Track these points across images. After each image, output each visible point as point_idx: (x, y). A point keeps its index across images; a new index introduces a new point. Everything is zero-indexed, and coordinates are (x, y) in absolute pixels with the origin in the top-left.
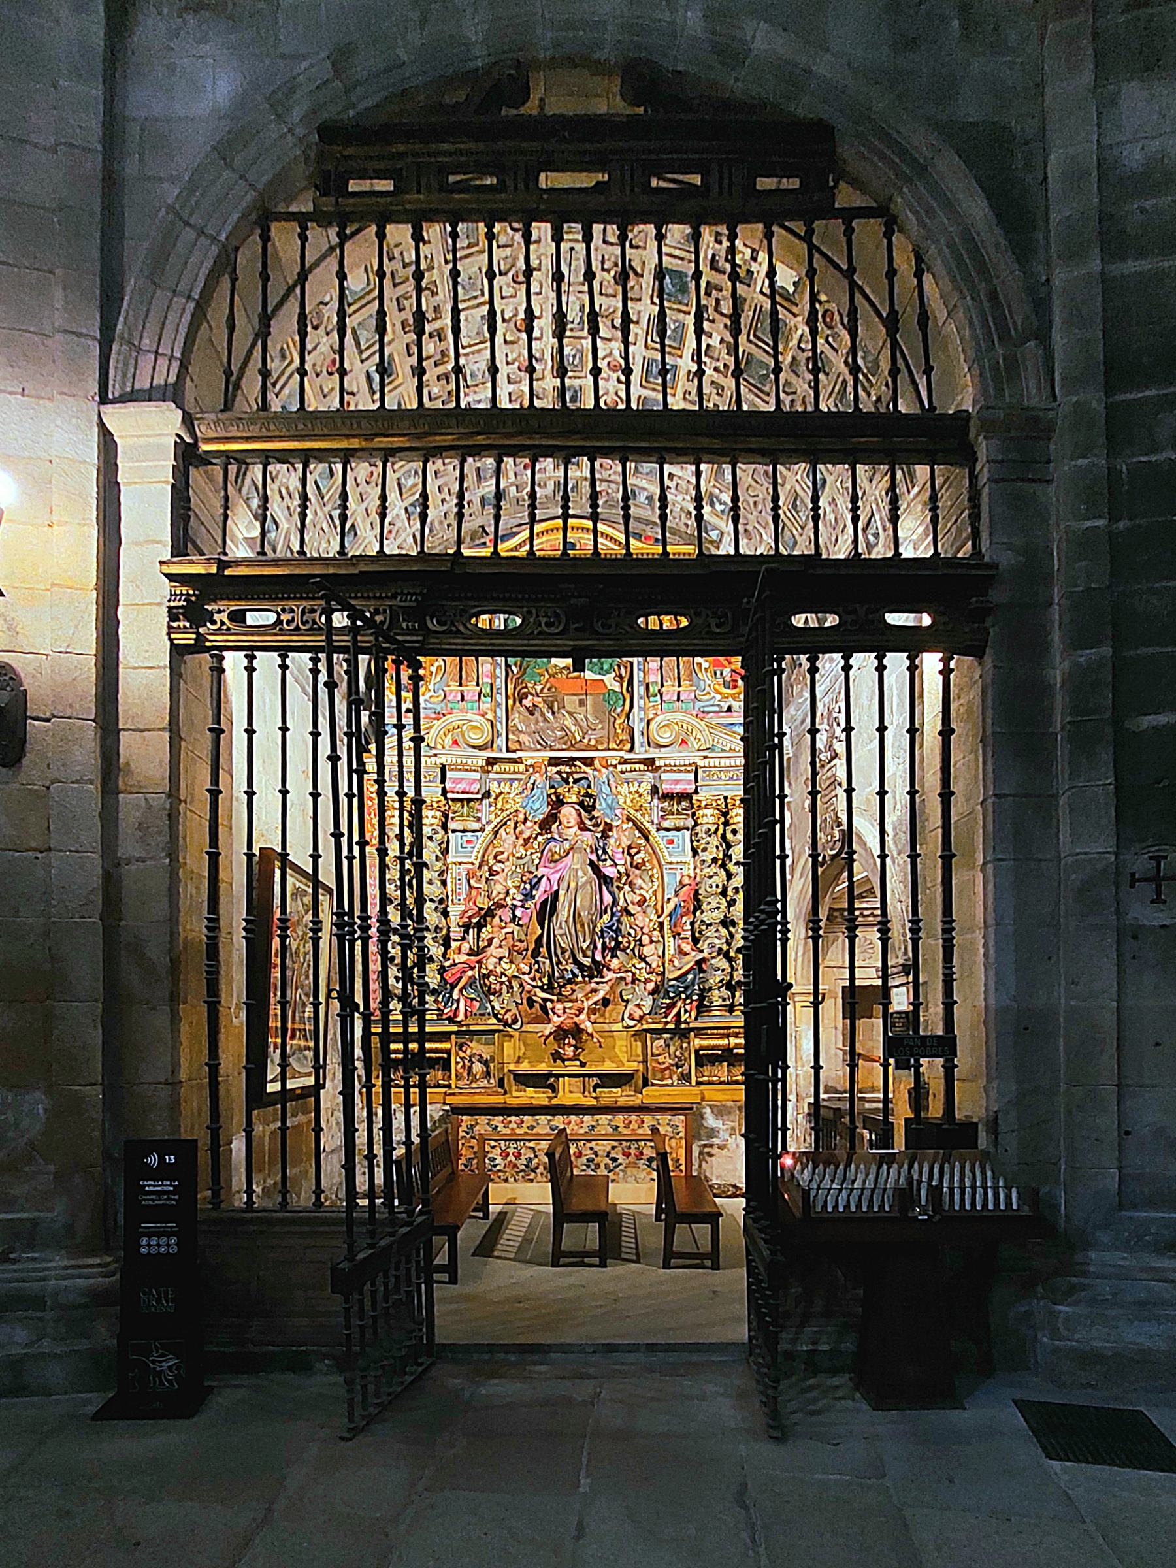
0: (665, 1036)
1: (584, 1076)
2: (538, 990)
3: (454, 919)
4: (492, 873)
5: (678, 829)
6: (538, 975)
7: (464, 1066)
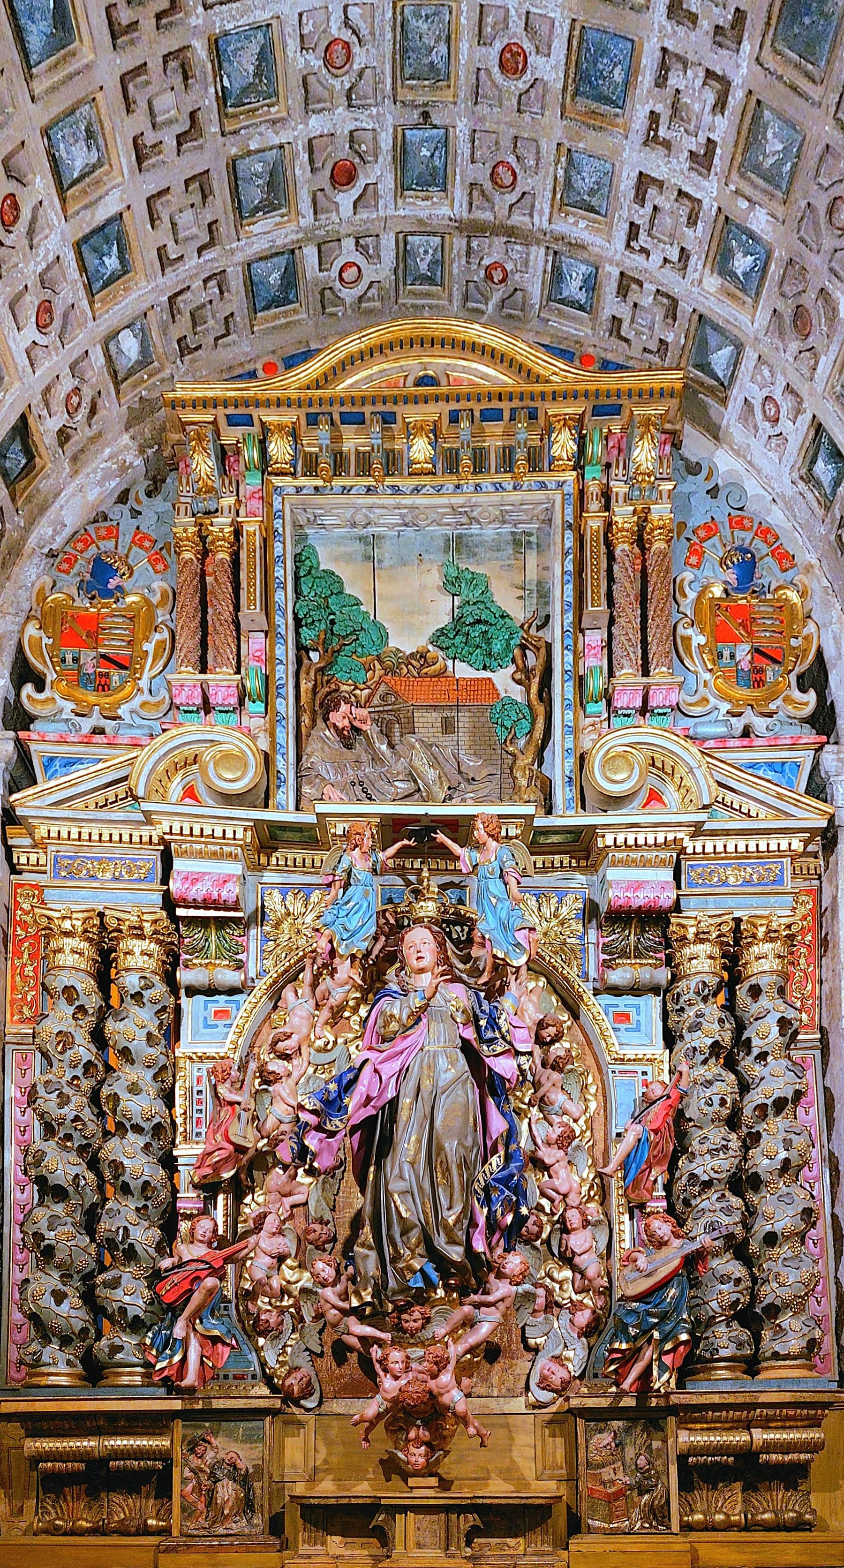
0: (617, 1424)
1: (447, 1509)
2: (352, 1321)
3: (184, 1175)
4: (268, 1079)
5: (636, 990)
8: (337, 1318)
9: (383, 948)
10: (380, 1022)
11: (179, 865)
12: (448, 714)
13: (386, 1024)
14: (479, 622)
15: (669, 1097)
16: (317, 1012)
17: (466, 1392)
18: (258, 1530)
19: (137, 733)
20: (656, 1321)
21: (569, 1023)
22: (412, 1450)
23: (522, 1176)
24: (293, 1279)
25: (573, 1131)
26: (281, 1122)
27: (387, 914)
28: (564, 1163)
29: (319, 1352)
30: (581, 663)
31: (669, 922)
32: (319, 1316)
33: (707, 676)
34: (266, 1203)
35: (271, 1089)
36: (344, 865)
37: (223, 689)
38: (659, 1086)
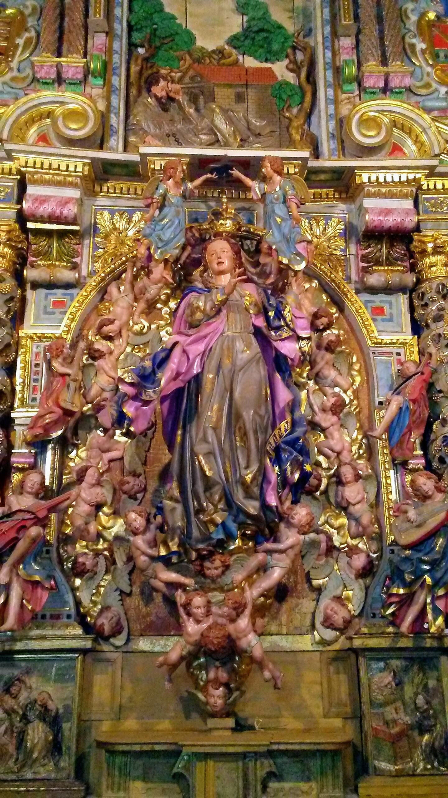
0: (396, 663)
2: (159, 566)
6: (160, 536)
7: (10, 730)
9: (189, 255)
11: (31, 190)
12: (240, 90)
13: (193, 314)
14: (262, 30)
15: (422, 373)
16: (135, 304)
17: (259, 631)
18: (64, 774)
19: (6, 97)
20: (427, 568)
21: (337, 315)
22: (212, 691)
23: (306, 439)
25: (344, 400)
26: (103, 390)
27: (194, 230)
28: (337, 427)
30: (337, 59)
31: (411, 240)
32: (130, 558)
33: (429, 69)
34: (89, 458)
36: (161, 191)
37: (73, 69)
38: (412, 364)
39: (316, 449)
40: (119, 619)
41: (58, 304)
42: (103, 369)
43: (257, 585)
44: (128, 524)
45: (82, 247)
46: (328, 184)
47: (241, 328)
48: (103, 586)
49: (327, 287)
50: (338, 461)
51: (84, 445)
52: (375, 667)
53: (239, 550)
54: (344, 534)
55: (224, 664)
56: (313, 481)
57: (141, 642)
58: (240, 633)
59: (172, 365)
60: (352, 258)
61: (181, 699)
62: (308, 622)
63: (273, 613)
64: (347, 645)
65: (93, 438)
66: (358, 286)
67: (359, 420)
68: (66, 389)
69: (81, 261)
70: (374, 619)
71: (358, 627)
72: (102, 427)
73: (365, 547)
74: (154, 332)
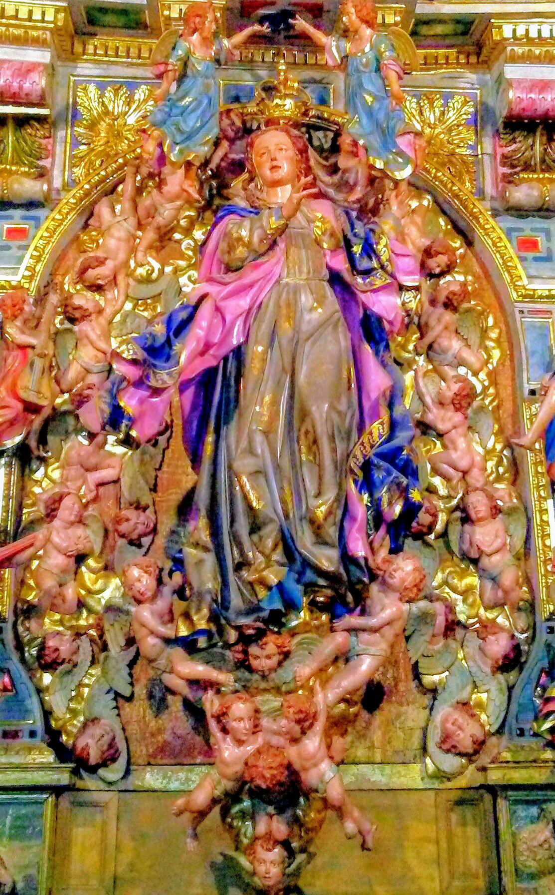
2: (178, 652)
6: (180, 606)
8: (158, 649)
9: (226, 155)
10: (223, 246)
13: (231, 249)
16: (140, 233)
17: (338, 758)
21: (462, 251)
23: (412, 450)
24: (97, 586)
25: (473, 388)
26: (88, 371)
29: (127, 693)
32: (131, 641)
34: (64, 480)
35: (76, 328)
39: (429, 466)
40: (114, 739)
41: (13, 233)
42: (87, 337)
43: (334, 683)
44: (127, 586)
45: (54, 142)
46: (448, 41)
47: (309, 273)
48: (87, 686)
49: (446, 207)
50: (464, 485)
51: (58, 460)
52: (523, 814)
53: (305, 627)
54: (474, 601)
55: (280, 811)
56: (423, 518)
57: (148, 776)
58: (307, 760)
59: (198, 331)
60: (487, 160)
61: (213, 865)
62: (416, 742)
63: (359, 728)
64: (479, 779)
65: (71, 448)
66: (497, 205)
67: (498, 420)
68: (27, 370)
69: (53, 164)
70: (521, 739)
71: (495, 751)
72: (86, 430)
73: (507, 623)
74: (169, 278)
